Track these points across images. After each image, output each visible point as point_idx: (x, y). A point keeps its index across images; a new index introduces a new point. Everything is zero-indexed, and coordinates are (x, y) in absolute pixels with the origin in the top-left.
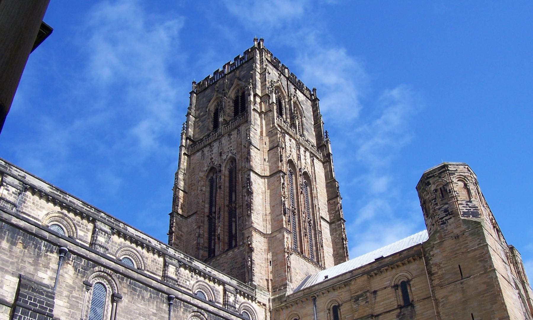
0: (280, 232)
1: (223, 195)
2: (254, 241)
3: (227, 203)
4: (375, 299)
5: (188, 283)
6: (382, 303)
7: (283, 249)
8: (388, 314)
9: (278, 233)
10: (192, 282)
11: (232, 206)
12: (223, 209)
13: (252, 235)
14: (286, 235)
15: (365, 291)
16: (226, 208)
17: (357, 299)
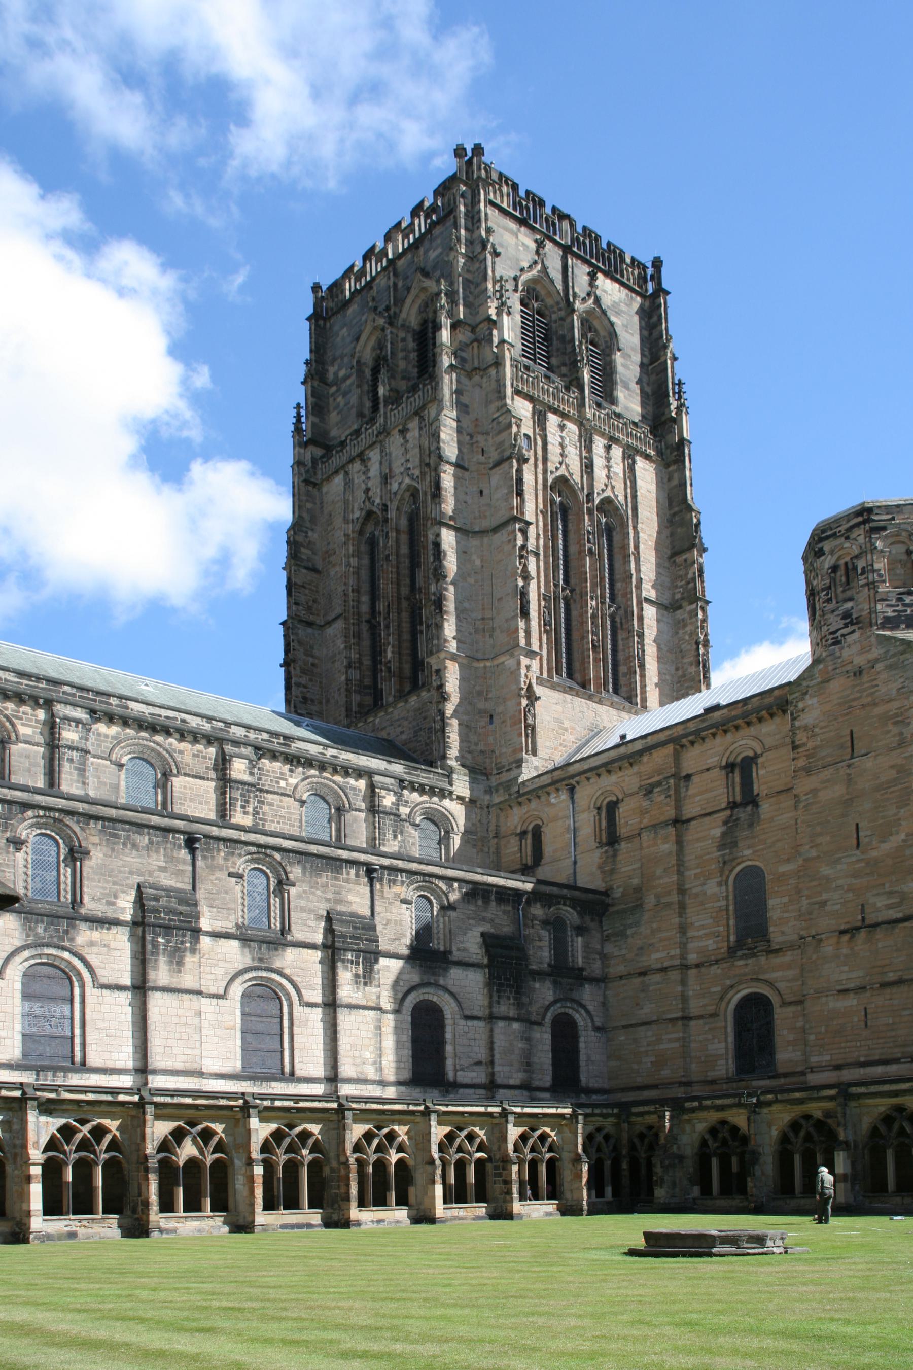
0: (512, 655)
1: (394, 576)
2: (450, 681)
3: (405, 591)
4: (687, 790)
5: (283, 784)
6: (698, 798)
7: (517, 691)
8: (707, 819)
9: (508, 657)
10: (293, 781)
11: (415, 599)
12: (395, 607)
13: (446, 668)
14: (524, 661)
15: (666, 775)
16: (405, 604)
17: (649, 791)
